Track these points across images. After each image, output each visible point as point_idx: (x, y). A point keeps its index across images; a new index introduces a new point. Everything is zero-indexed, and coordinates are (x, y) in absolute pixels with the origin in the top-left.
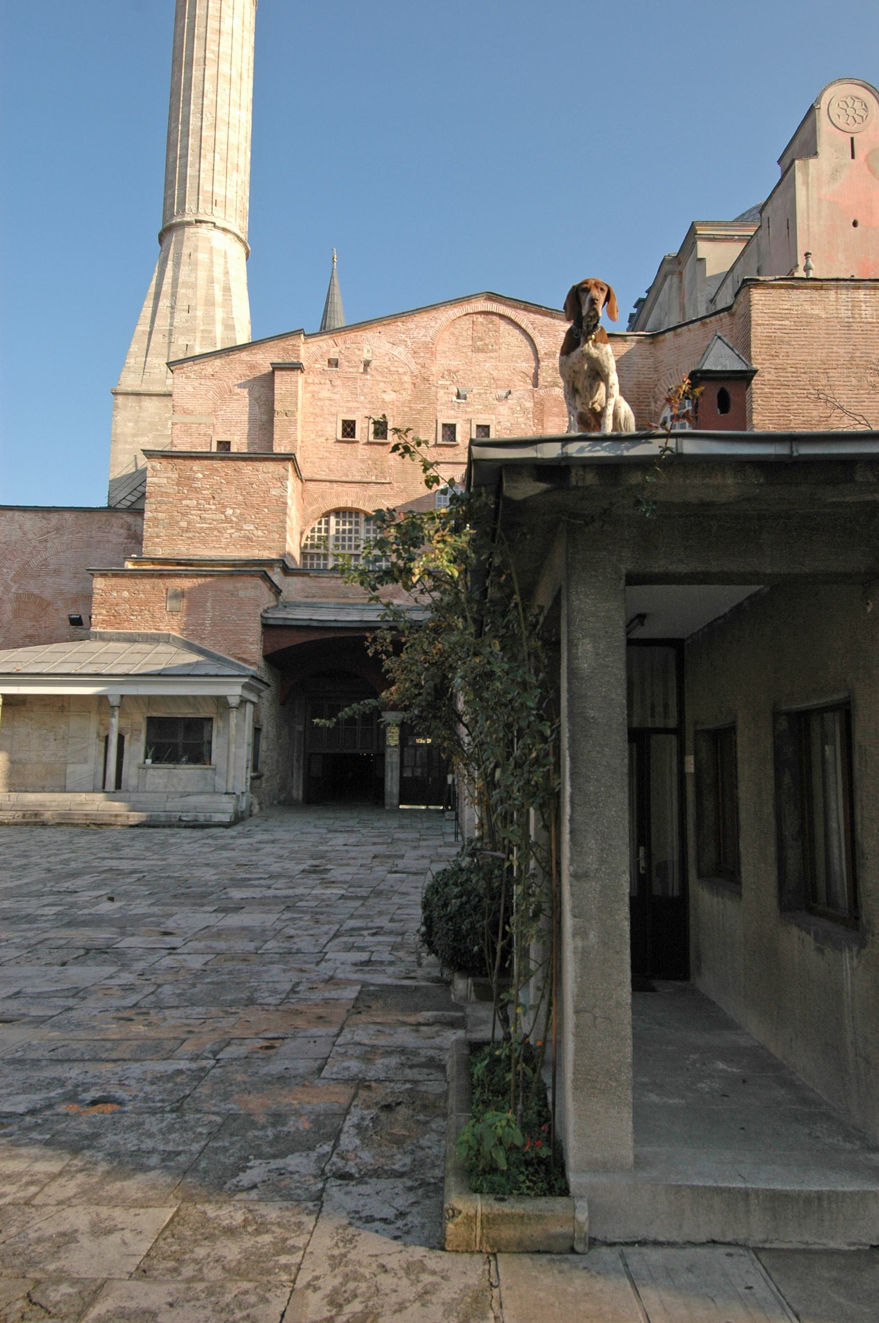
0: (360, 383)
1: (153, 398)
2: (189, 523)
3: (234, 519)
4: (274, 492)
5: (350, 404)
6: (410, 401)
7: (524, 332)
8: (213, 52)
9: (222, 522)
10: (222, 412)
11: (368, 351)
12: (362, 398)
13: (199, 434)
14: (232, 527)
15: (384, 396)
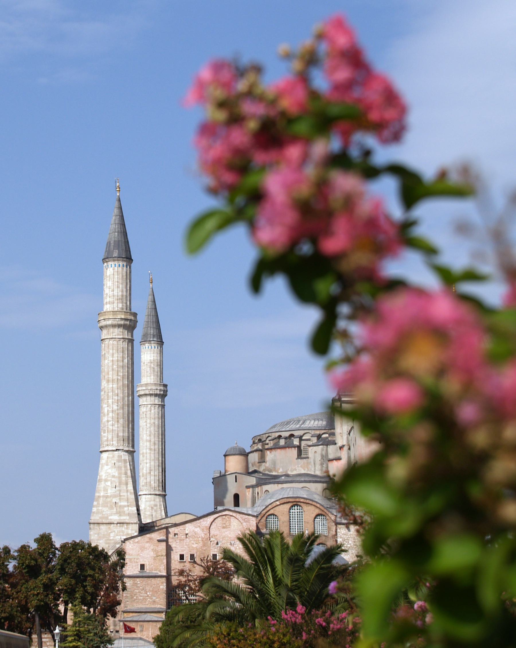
0: (185, 541)
1: (104, 524)
2: (137, 597)
3: (150, 596)
4: (161, 587)
5: (182, 549)
6: (201, 547)
7: (239, 521)
8: (120, 375)
9: (146, 597)
10: (142, 554)
11: (187, 530)
12: (186, 546)
13: (135, 562)
14: (149, 598)
15: (193, 545)
